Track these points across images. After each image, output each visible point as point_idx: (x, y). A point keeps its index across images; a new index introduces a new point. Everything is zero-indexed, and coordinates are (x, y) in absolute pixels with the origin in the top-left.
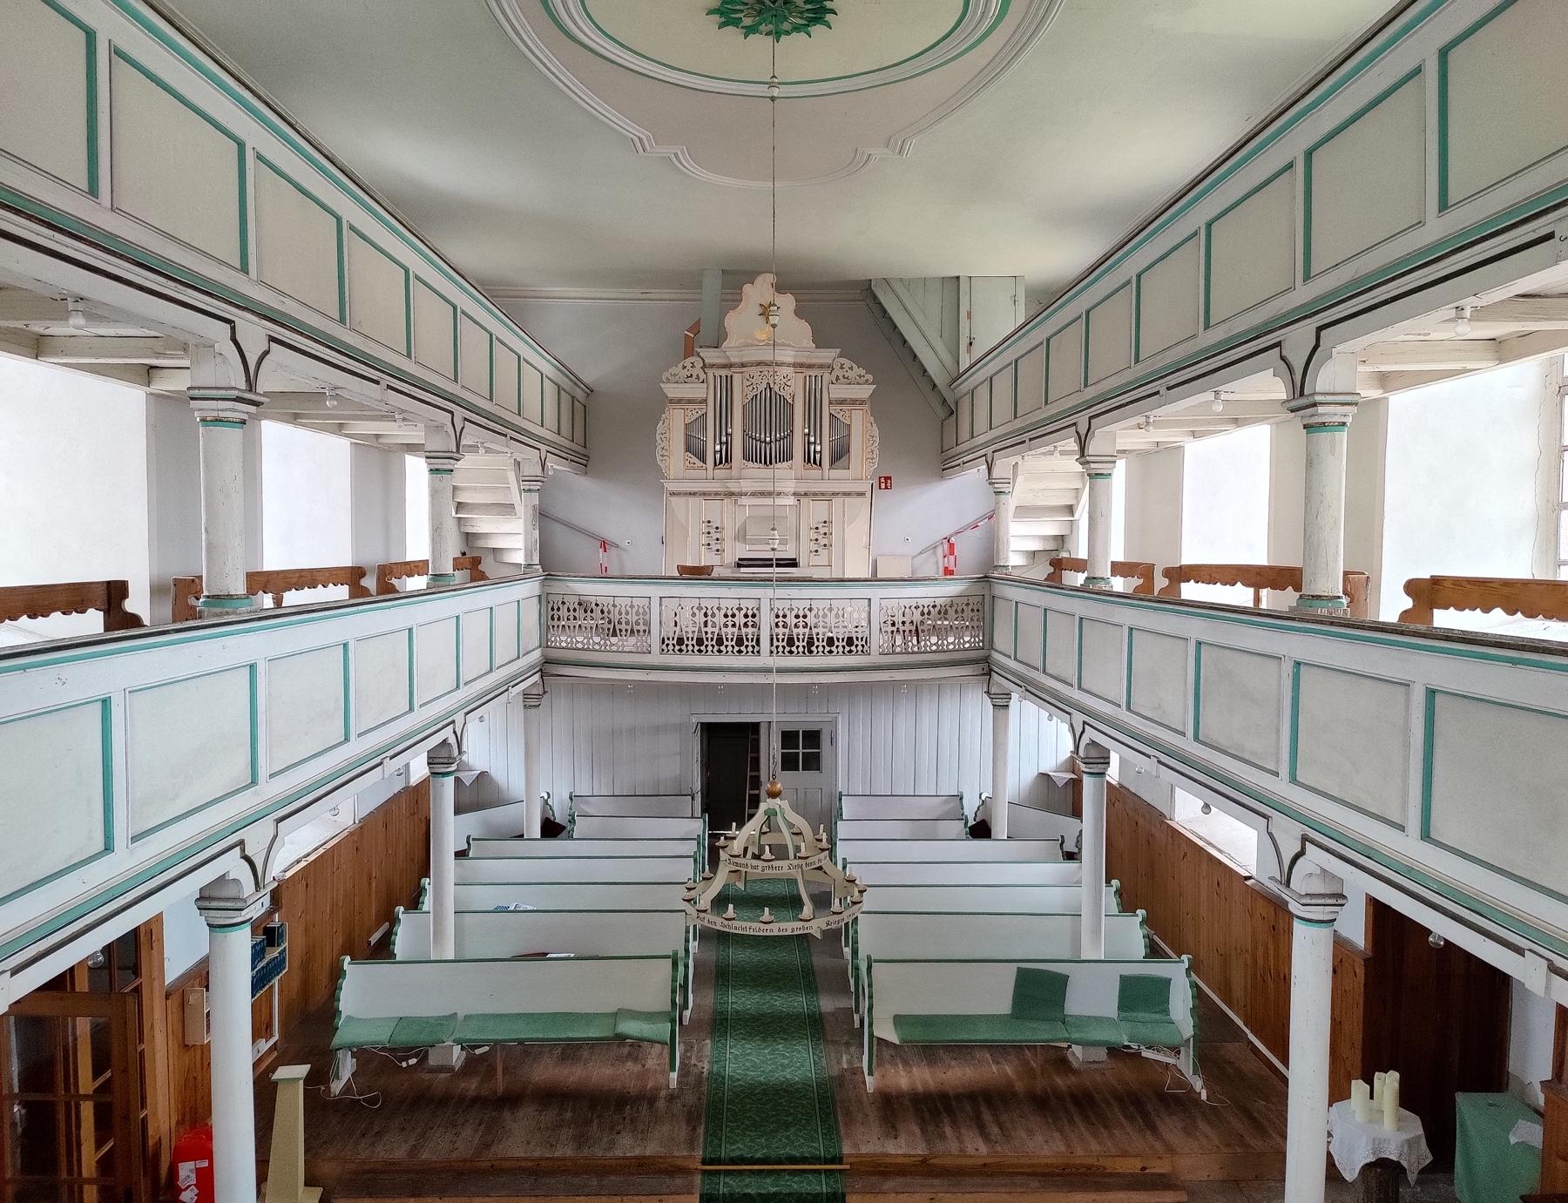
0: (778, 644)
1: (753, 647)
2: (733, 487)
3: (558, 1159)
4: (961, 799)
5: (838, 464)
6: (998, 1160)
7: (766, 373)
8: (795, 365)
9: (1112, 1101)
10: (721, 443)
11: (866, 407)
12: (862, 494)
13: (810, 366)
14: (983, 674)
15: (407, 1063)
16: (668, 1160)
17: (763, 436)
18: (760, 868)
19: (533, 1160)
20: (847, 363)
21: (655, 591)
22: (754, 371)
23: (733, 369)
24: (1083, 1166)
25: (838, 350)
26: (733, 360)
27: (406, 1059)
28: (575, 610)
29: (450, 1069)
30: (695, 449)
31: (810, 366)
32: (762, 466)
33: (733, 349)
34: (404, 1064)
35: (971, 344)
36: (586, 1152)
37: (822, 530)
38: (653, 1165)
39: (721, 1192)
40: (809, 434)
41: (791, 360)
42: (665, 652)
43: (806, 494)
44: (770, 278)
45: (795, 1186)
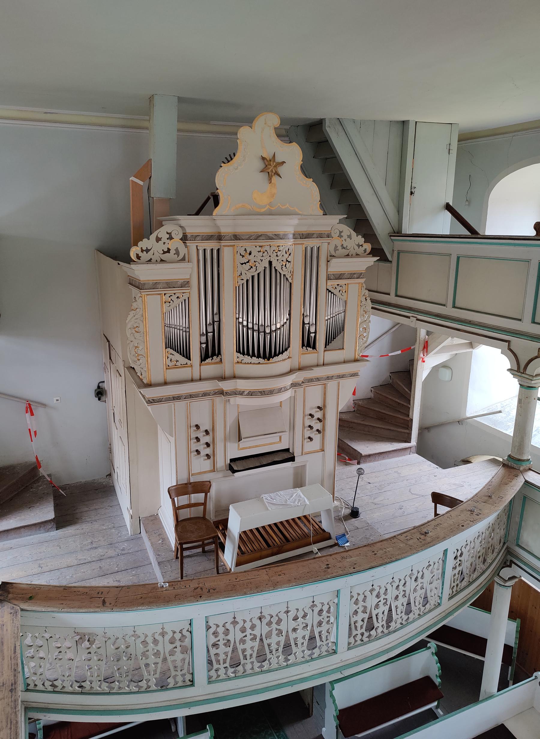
0: (356, 632)
2: (226, 386)
5: (334, 344)
7: (267, 248)
11: (362, 281)
13: (308, 236)
22: (249, 245)
23: (223, 243)
31: (308, 236)
32: (261, 360)
35: (412, 193)
42: (213, 679)
44: (274, 120)
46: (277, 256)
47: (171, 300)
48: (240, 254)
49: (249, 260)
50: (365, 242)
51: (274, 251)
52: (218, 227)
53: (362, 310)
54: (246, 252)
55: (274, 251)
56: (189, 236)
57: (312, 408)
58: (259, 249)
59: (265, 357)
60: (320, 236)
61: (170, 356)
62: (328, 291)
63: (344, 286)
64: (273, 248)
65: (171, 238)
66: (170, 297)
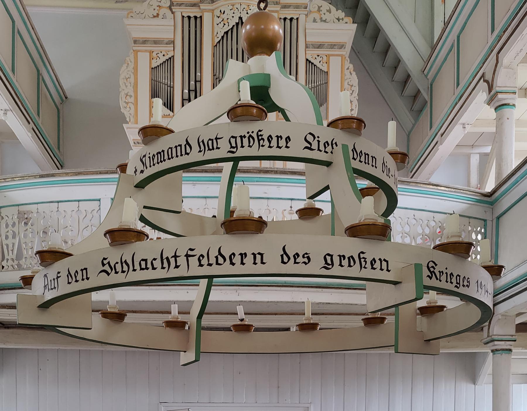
7: (238, 6)
10: (189, 91)
46: (247, 13)
47: (158, 57)
48: (217, 16)
49: (223, 19)
50: (345, 16)
51: (244, 8)
54: (221, 13)
55: (244, 8)
56: (175, 3)
58: (231, 7)
62: (308, 62)
63: (325, 58)
64: (243, 6)
66: (157, 54)
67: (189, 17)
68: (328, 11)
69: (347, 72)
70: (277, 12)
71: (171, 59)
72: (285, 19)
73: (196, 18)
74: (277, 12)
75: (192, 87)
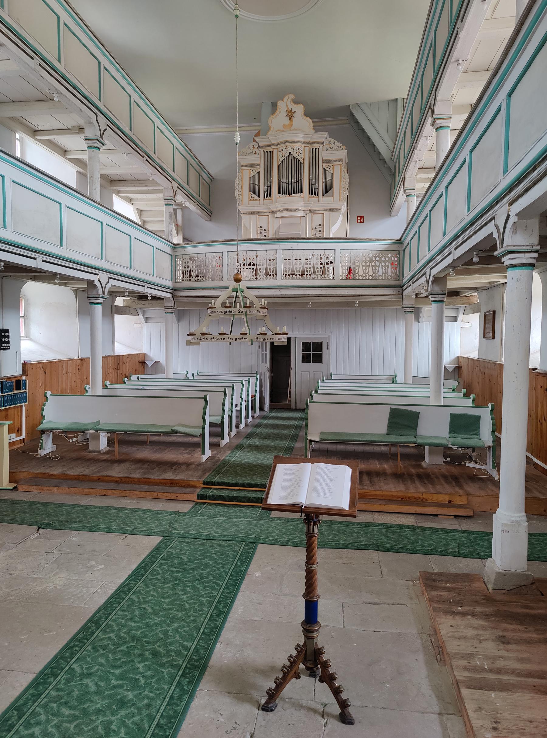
1: (273, 275)
3: (131, 478)
4: (396, 377)
6: (364, 491)
7: (289, 147)
8: (304, 143)
9: (440, 478)
10: (267, 187)
12: (340, 210)
13: (313, 143)
14: (399, 294)
15: (72, 440)
16: (186, 482)
17: (287, 180)
18: (223, 312)
19: (119, 477)
20: (332, 140)
21: (224, 249)
22: (283, 146)
23: (273, 147)
24: (413, 497)
25: (327, 133)
26: (273, 142)
27: (72, 438)
28: (188, 262)
29: (99, 452)
30: (254, 190)
31: (313, 143)
33: (273, 137)
34: (71, 440)
36: (146, 476)
37: (318, 230)
38: (177, 483)
39: (208, 494)
40: (312, 180)
41: (302, 140)
43: (310, 211)
44: (292, 96)
45: (248, 495)
52: (270, 141)
53: (342, 178)
57: (317, 226)
59: (289, 194)
60: (318, 143)
61: (251, 195)
63: (332, 166)
65: (253, 147)
67: (267, 152)
68: (333, 143)
69: (343, 173)
70: (308, 146)
71: (259, 172)
72: (313, 149)
73: (270, 152)
74: (308, 146)
75: (269, 185)
